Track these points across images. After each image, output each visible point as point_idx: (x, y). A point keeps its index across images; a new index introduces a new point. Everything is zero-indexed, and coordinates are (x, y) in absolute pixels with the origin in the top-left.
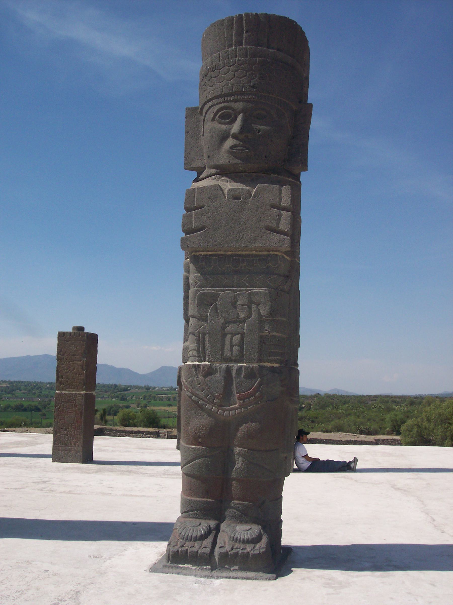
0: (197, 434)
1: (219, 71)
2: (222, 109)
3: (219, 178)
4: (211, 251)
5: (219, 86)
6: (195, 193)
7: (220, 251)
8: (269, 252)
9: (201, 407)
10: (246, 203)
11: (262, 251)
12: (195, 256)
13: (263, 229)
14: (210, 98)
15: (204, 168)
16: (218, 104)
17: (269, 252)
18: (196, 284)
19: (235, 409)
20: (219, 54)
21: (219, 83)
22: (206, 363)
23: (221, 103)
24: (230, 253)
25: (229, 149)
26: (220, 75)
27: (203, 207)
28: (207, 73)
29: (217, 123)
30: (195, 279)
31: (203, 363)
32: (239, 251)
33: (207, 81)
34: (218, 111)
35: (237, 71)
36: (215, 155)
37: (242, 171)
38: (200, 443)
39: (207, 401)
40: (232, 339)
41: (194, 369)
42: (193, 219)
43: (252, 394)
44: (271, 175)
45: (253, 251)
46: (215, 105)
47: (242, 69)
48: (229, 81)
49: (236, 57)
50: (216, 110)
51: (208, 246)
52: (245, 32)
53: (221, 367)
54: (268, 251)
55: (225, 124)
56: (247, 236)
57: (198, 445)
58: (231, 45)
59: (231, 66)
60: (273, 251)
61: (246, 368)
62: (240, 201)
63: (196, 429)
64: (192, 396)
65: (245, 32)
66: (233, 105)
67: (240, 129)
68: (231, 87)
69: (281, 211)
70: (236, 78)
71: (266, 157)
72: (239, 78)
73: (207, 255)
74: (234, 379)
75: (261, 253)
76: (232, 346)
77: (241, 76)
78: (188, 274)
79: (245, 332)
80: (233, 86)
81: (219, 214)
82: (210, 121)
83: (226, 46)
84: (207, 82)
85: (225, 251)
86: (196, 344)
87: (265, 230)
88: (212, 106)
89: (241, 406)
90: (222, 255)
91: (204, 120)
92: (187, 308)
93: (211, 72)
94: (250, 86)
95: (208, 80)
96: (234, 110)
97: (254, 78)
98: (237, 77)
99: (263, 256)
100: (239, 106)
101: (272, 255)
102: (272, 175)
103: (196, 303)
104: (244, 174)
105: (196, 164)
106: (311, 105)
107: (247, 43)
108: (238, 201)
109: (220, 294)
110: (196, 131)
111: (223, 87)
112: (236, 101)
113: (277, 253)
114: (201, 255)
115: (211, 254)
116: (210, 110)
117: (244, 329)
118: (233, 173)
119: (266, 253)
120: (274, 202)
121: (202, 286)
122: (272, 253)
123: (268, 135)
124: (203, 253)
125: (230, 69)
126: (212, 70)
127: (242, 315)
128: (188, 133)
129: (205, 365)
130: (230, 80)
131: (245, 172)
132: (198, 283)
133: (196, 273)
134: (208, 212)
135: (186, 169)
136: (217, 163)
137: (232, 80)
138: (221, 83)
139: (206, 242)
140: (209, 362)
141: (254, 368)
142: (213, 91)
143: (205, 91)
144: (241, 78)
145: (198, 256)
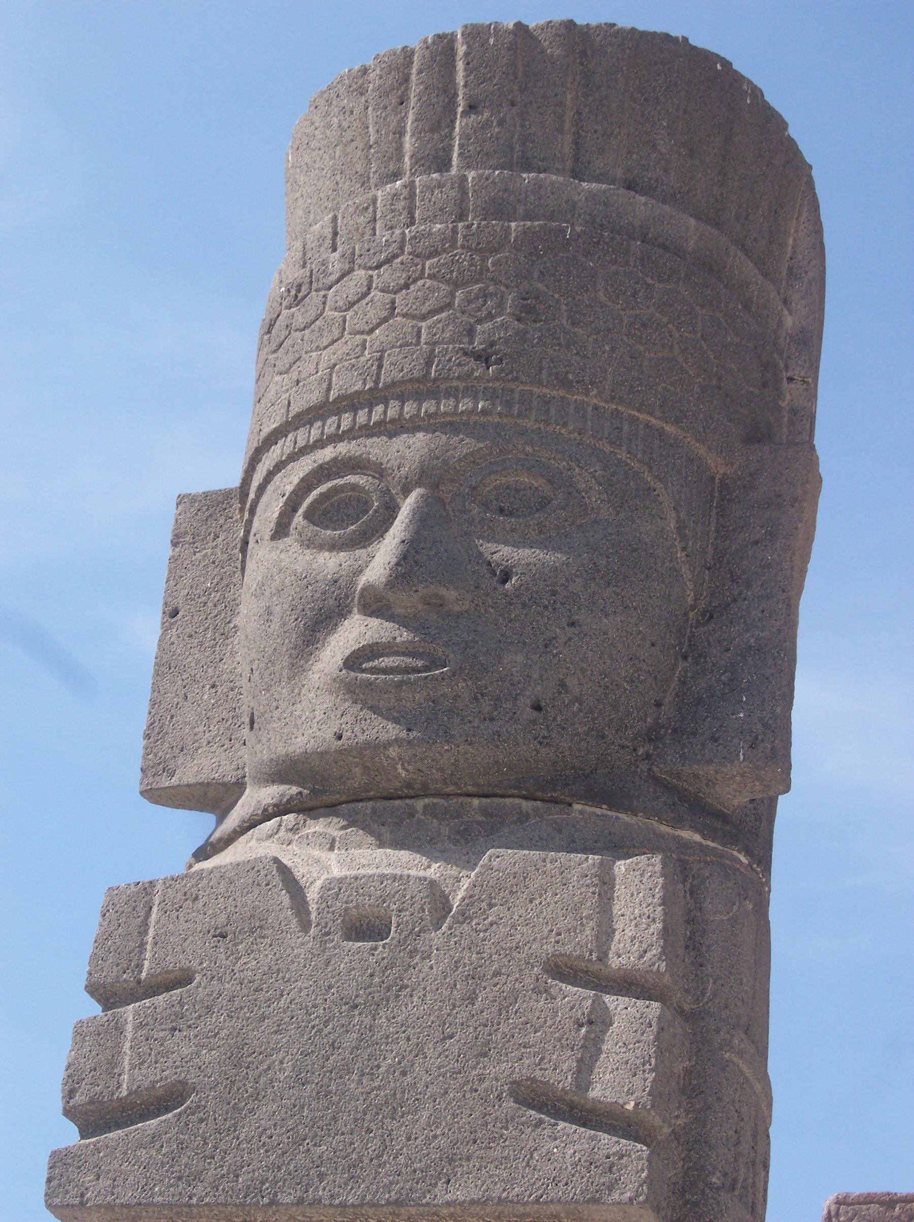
1: (325, 296)
2: (322, 473)
3: (294, 830)
6: (151, 908)
10: (413, 953)
13: (499, 1098)
15: (238, 787)
21: (318, 348)
23: (320, 444)
25: (341, 671)
26: (328, 312)
27: (183, 979)
29: (296, 547)
34: (306, 485)
35: (406, 286)
37: (409, 785)
44: (570, 805)
47: (432, 277)
48: (365, 337)
50: (296, 481)
51: (190, 1198)
52: (460, 109)
55: (334, 546)
56: (409, 1139)
62: (381, 943)
65: (460, 109)
67: (394, 560)
69: (608, 999)
71: (537, 708)
72: (414, 317)
77: (425, 309)
80: (381, 359)
81: (263, 1018)
82: (267, 537)
84: (270, 357)
95: (274, 347)
96: (379, 471)
97: (490, 316)
102: (577, 807)
104: (420, 804)
107: (468, 162)
111: (335, 365)
116: (270, 488)
120: (568, 949)
123: (554, 593)
125: (375, 277)
128: (175, 613)
130: (372, 331)
131: (425, 792)
135: (153, 795)
138: (325, 348)
142: (288, 394)
144: (424, 318)
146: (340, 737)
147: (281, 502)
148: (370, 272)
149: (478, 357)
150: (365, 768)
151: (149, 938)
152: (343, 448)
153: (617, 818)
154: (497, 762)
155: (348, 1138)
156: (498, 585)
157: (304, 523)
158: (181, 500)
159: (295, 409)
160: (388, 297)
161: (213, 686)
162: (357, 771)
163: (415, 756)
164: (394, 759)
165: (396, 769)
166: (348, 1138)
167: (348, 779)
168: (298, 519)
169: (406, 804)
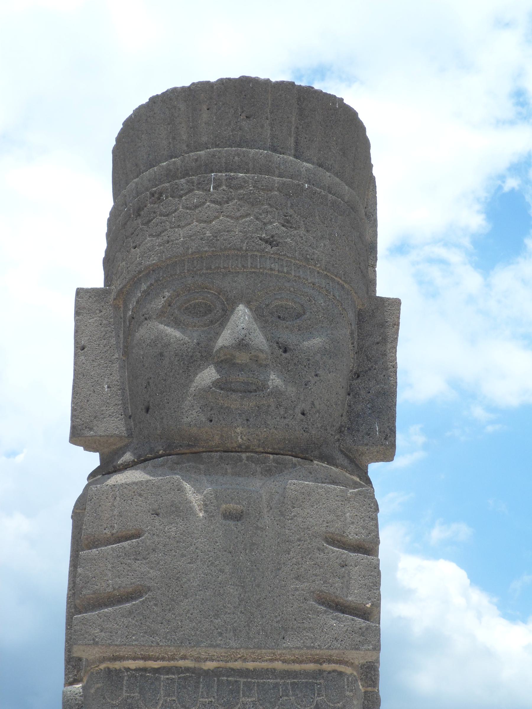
4: (156, 659)
7: (184, 658)
8: (321, 664)
11: (301, 662)
12: (109, 671)
17: (321, 664)
24: (210, 665)
32: (236, 660)
37: (240, 446)
44: (312, 461)
45: (276, 660)
54: (316, 662)
60: (330, 661)
71: (303, 414)
73: (144, 670)
75: (297, 667)
77: (238, 214)
85: (198, 659)
90: (187, 669)
94: (261, 239)
99: (306, 674)
101: (329, 672)
102: (315, 462)
104: (244, 456)
114: (128, 669)
115: (156, 667)
118: (217, 451)
119: (311, 667)
120: (332, 530)
122: (327, 667)
123: (309, 360)
124: (132, 664)
128: (83, 348)
131: (247, 449)
138: (184, 227)
145: (118, 672)
149: (266, 242)
150: (222, 436)
153: (331, 468)
154: (285, 439)
155: (232, 616)
156: (283, 354)
158: (80, 292)
162: (217, 437)
163: (249, 432)
164: (238, 433)
165: (237, 438)
167: (210, 441)
169: (238, 455)
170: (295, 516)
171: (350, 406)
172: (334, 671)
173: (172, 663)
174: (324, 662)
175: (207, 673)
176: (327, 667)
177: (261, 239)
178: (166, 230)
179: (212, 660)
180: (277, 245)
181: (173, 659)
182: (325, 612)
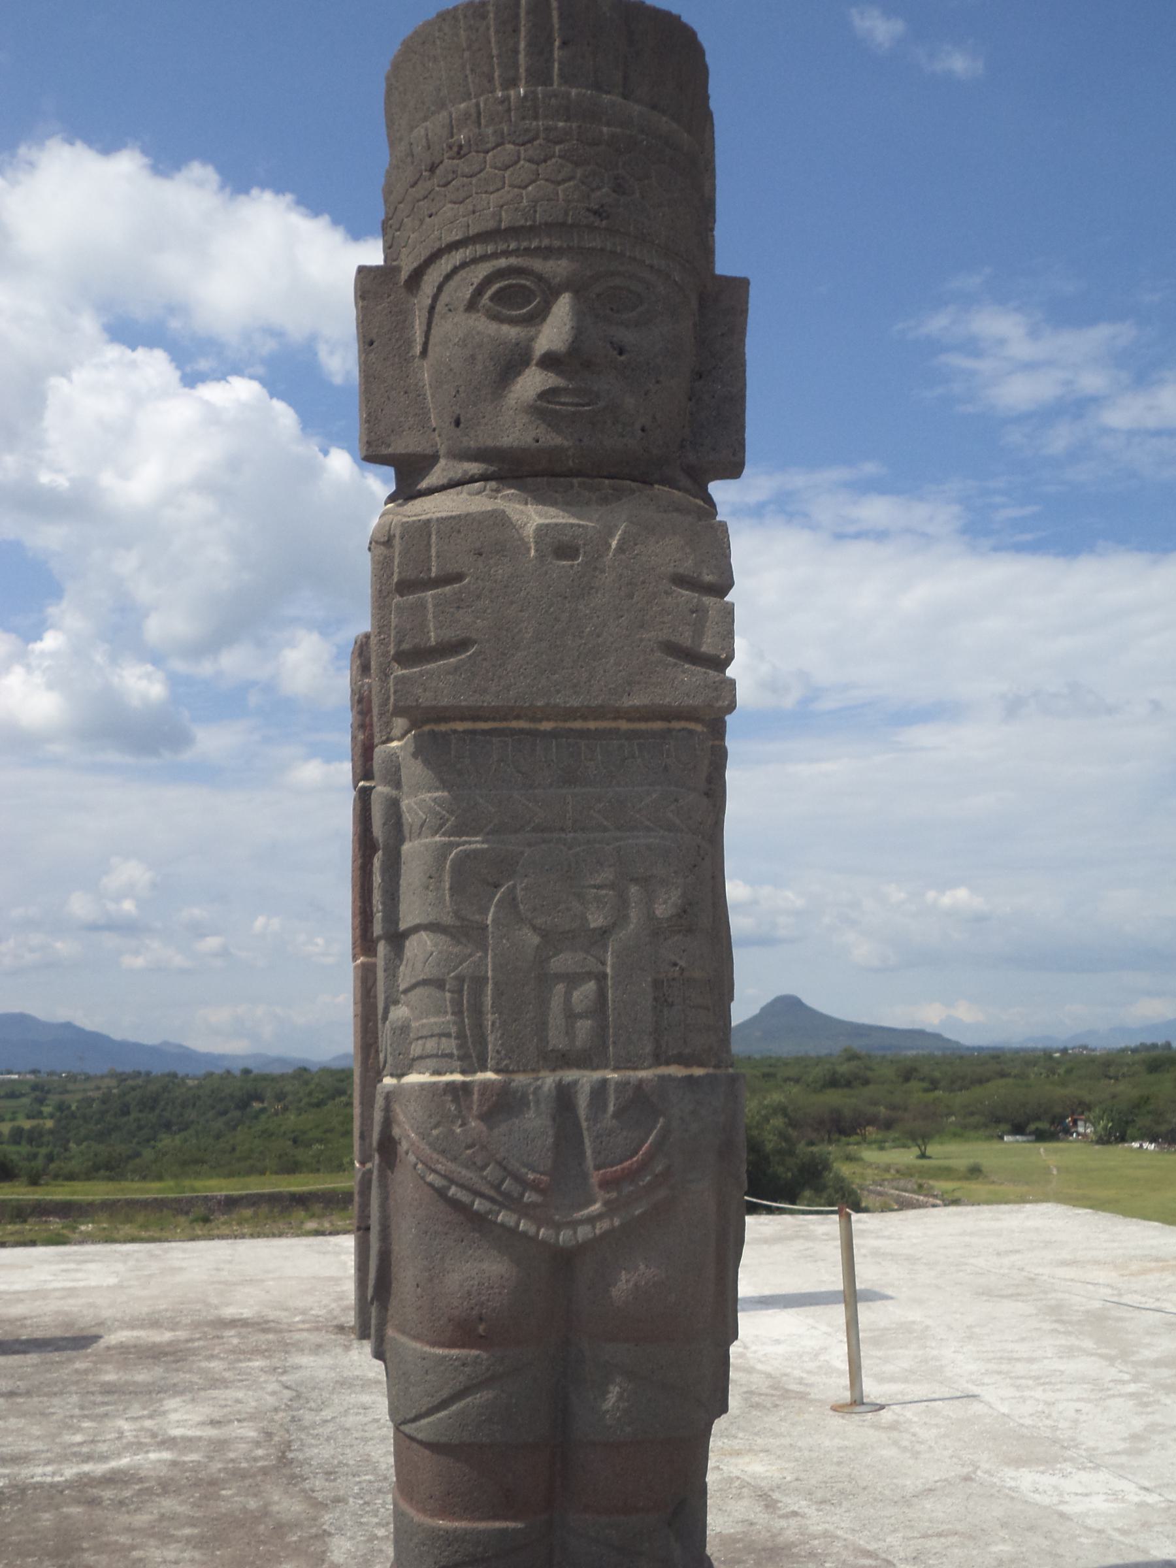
0: (472, 1308)
1: (485, 158)
2: (499, 274)
3: (498, 491)
5: (488, 203)
6: (430, 536)
9: (479, 1223)
10: (595, 569)
12: (433, 734)
13: (652, 650)
14: (457, 238)
15: (433, 459)
16: (485, 258)
18: (441, 826)
19: (591, 1220)
20: (478, 105)
21: (486, 192)
22: (490, 1075)
23: (495, 255)
26: (488, 169)
27: (459, 577)
28: (437, 162)
29: (483, 319)
30: (438, 809)
31: (480, 1076)
32: (575, 719)
33: (439, 186)
35: (545, 161)
36: (484, 417)
38: (481, 1337)
39: (500, 1199)
40: (568, 995)
41: (450, 1099)
42: (430, 616)
43: (643, 1166)
46: (475, 261)
47: (560, 157)
48: (521, 190)
49: (536, 118)
50: (481, 277)
51: (483, 702)
52: (557, 43)
53: (539, 1088)
55: (512, 321)
56: (605, 671)
57: (472, 1346)
58: (512, 83)
59: (523, 145)
61: (622, 1085)
62: (576, 562)
63: (469, 1293)
64: (449, 1188)
65: (557, 43)
66: (537, 265)
67: (570, 340)
68: (528, 208)
69: (705, 599)
70: (542, 182)
71: (643, 430)
72: (553, 182)
73: (473, 732)
74: (584, 1124)
75: (642, 726)
76: (571, 1016)
77: (560, 178)
78: (394, 792)
79: (609, 970)
80: (534, 206)
81: (512, 603)
82: (462, 308)
83: (497, 83)
84: (437, 189)
86: (449, 1017)
87: (658, 654)
88: (464, 265)
89: (611, 1208)
91: (432, 309)
92: (393, 899)
93: (453, 158)
94: (588, 210)
95: (443, 181)
96: (540, 278)
97: (599, 188)
98: (547, 180)
100: (558, 268)
101: (680, 730)
102: (656, 486)
103: (447, 886)
104: (575, 481)
105: (407, 443)
106: (739, 286)
107: (566, 79)
108: (570, 563)
109: (522, 853)
110: (397, 340)
111: (502, 206)
112: (546, 253)
113: (691, 726)
114: (455, 732)
116: (457, 278)
117: (604, 963)
120: (681, 570)
121: (458, 831)
124: (460, 726)
125: (522, 152)
126: (458, 153)
127: (596, 920)
128: (371, 343)
129: (486, 1085)
130: (526, 187)
131: (578, 474)
132: (448, 820)
133: (437, 789)
134: (479, 597)
136: (490, 443)
137: (530, 188)
138: (492, 193)
139: (475, 692)
140: (497, 1071)
141: (644, 1085)
142: (465, 219)
143: (430, 216)
144: (559, 183)
145: (445, 735)
146: (537, 441)
147: (471, 289)
148: (517, 148)
149: (595, 213)
151: (433, 552)
152: (513, 261)
155: (570, 671)
157: (490, 304)
159: (472, 232)
160: (534, 167)
161: (406, 393)
166: (570, 671)
168: (485, 299)
170: (637, 554)
171: (691, 414)
172: (683, 729)
173: (504, 725)
174: (673, 719)
175: (545, 735)
176: (677, 725)
177: (588, 210)
178: (471, 196)
179: (548, 719)
180: (607, 217)
181: (505, 719)
182: (676, 664)
